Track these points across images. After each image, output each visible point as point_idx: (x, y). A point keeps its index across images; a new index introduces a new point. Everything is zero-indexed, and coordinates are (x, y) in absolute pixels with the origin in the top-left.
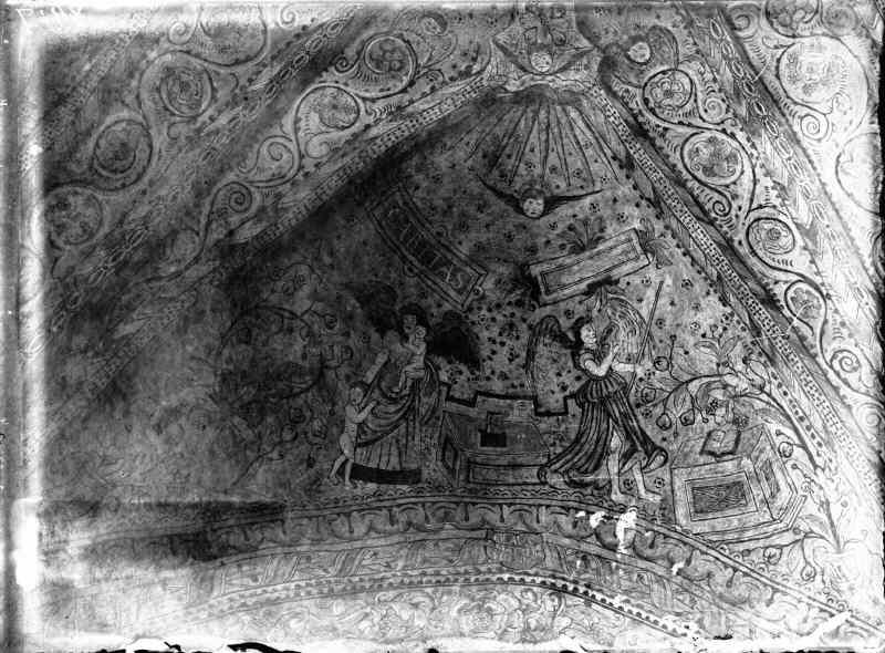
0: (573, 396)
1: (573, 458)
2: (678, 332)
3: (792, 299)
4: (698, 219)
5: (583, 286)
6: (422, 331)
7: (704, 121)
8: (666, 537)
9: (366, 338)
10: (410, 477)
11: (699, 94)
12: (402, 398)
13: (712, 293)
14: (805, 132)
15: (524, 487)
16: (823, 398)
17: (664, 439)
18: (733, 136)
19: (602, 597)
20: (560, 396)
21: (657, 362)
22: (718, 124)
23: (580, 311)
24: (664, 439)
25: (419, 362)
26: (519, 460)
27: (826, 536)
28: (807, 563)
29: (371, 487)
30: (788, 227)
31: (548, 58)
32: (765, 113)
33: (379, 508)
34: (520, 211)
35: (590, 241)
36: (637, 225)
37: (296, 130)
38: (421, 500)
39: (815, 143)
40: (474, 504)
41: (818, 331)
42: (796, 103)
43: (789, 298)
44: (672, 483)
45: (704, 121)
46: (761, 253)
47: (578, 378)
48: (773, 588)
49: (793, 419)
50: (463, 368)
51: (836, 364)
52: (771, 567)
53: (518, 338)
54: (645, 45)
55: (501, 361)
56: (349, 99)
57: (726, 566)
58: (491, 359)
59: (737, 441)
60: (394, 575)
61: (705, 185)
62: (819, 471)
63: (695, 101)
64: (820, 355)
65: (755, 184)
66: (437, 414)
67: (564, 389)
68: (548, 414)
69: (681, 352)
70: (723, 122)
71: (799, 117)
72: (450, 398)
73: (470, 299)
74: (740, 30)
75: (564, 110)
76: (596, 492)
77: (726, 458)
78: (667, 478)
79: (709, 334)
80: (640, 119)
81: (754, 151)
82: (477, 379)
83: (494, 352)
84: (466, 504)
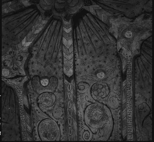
7: (53, 115)
11: (56, 106)
14: (84, 135)
18: (59, 126)
22: (57, 119)
31: (8, 72)
32: (71, 125)
42: (85, 124)
45: (53, 115)
54: (48, 80)
63: (54, 107)
70: (58, 119)
71: (84, 130)
74: (80, 90)
75: (10, 90)
80: (32, 105)
81: (63, 135)
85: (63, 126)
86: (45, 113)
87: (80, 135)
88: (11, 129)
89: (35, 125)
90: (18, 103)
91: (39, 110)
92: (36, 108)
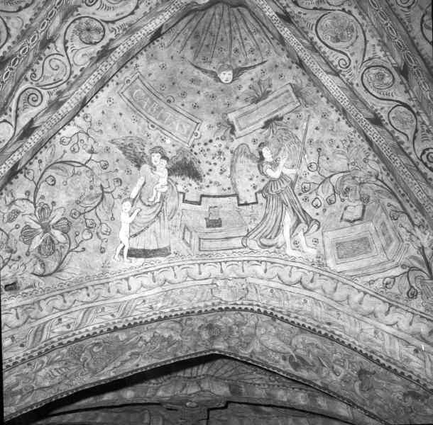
0: (261, 192)
1: (262, 230)
2: (322, 147)
3: (393, 118)
4: (328, 73)
5: (262, 123)
6: (164, 162)
7: (330, 5)
8: (320, 275)
9: (129, 172)
10: (163, 252)
12: (155, 204)
13: (341, 119)
15: (234, 250)
16: (415, 181)
17: (317, 214)
18: (350, 13)
19: (281, 315)
20: (253, 194)
21: (310, 166)
22: (339, 6)
23: (261, 139)
24: (317, 214)
25: (164, 181)
26: (230, 235)
27: (424, 269)
28: (412, 287)
29: (141, 260)
30: (391, 72)
33: (146, 273)
34: (218, 80)
35: (263, 94)
36: (294, 82)
37: (66, 49)
38: (172, 265)
39: (406, 10)
40: (204, 264)
41: (411, 137)
43: (392, 121)
44: (323, 243)
46: (371, 91)
47: (263, 180)
48: (390, 304)
49: (399, 197)
50: (191, 181)
51: (424, 158)
52: (388, 290)
53: (224, 159)
55: (215, 176)
56: (97, 23)
57: (359, 291)
58: (208, 174)
59: (364, 211)
60: (155, 314)
61: (332, 49)
62: (417, 229)
64: (413, 153)
65: (366, 44)
66: (178, 211)
67: (255, 188)
68: (246, 204)
69: (325, 158)
70: (342, 4)
72: (185, 201)
73: (192, 140)
75: (238, 10)
76: (277, 250)
77: (356, 223)
78: (320, 238)
79: (341, 145)
80: (288, 10)
81: (364, 21)
82: (201, 188)
83: (210, 170)
84: (199, 264)
85: (356, 10)
86: (315, 9)
87: (392, 5)
88: (276, 66)
89: (310, 35)
90: (264, 15)
91: (303, 11)
92: (297, 10)
